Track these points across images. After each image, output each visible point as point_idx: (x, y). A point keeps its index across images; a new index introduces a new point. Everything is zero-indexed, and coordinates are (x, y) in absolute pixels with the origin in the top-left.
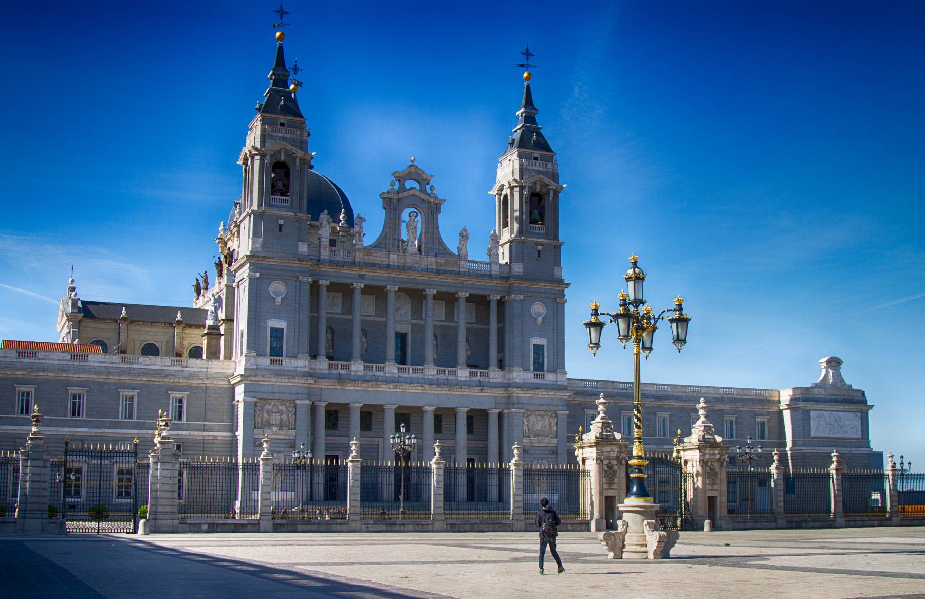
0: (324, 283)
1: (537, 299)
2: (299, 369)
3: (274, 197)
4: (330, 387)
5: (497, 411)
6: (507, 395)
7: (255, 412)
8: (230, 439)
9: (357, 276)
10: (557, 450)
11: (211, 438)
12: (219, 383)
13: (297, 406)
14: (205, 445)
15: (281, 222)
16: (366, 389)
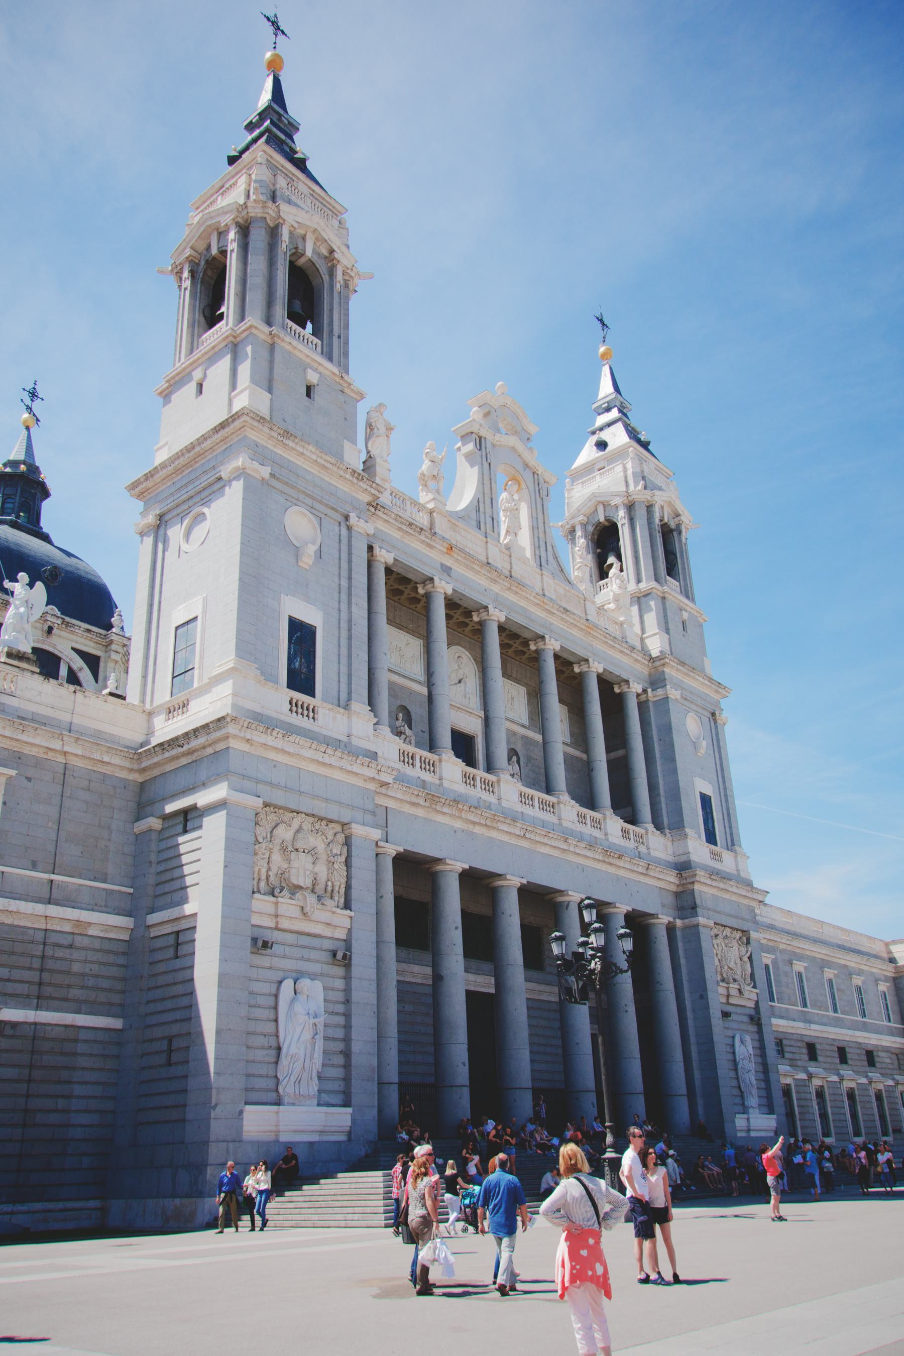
0: (384, 556)
1: (692, 706)
2: (355, 741)
3: (291, 323)
4: (407, 809)
5: (664, 919)
6: (673, 888)
7: (257, 842)
8: (125, 936)
9: (439, 567)
10: (759, 1019)
11: (67, 928)
12: (106, 759)
13: (355, 842)
14: (49, 952)
15: (313, 377)
16: (470, 827)
